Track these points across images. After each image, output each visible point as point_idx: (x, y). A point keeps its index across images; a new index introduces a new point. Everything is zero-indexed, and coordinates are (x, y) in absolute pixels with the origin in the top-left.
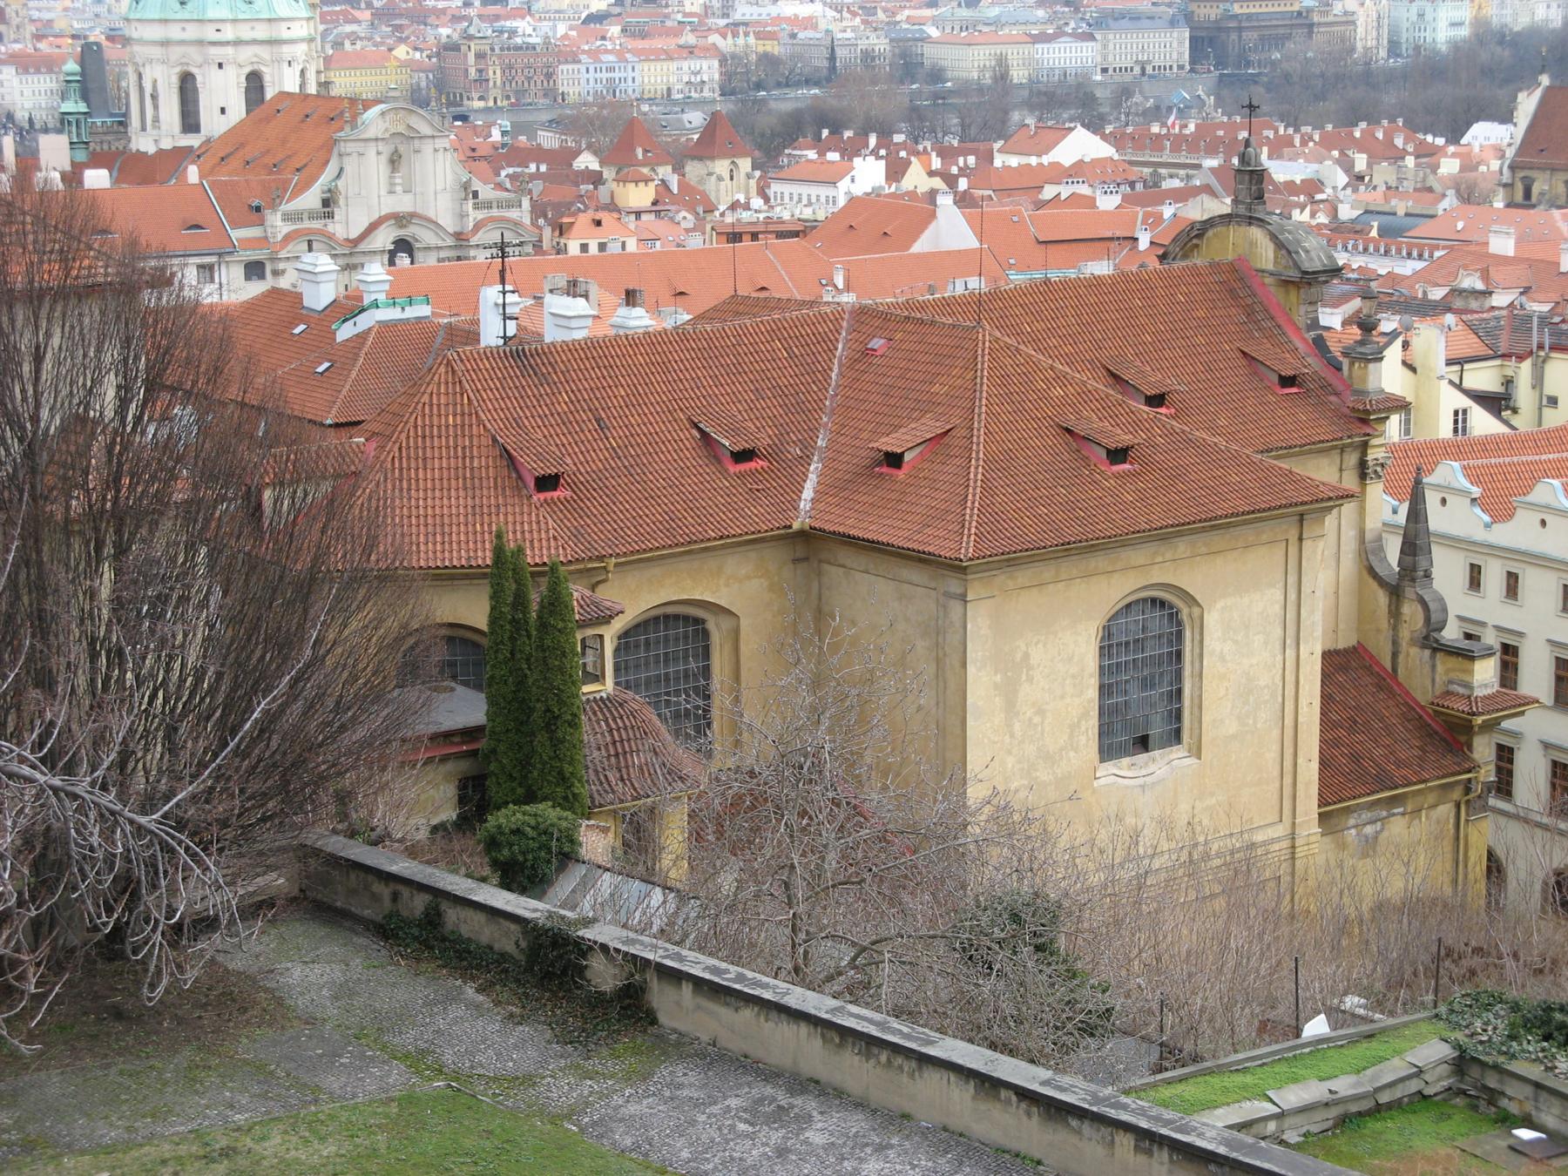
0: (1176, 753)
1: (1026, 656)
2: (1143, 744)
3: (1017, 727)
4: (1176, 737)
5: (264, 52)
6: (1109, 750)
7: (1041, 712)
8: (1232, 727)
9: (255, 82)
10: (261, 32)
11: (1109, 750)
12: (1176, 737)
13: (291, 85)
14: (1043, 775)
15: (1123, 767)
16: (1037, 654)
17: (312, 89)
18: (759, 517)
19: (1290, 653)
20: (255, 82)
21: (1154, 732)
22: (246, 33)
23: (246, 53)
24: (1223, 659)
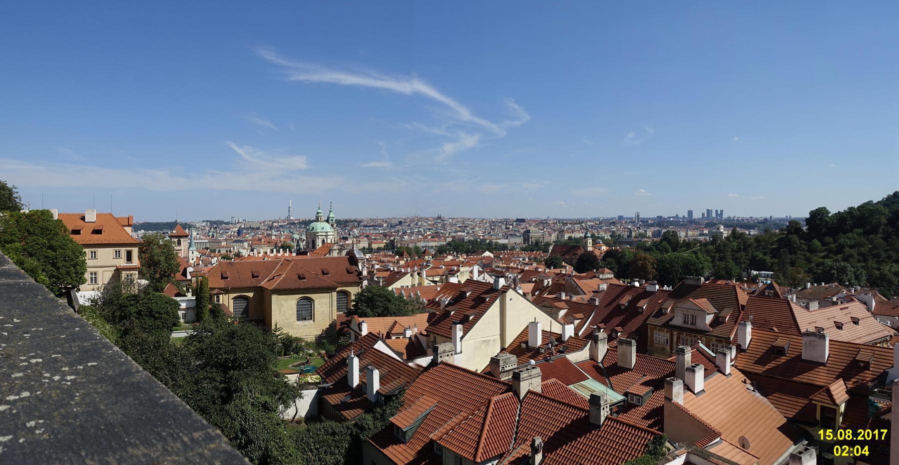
0: (311, 321)
1: (283, 304)
2: (305, 319)
3: (281, 314)
4: (311, 319)
5: (325, 237)
6: (297, 320)
7: (286, 313)
8: (321, 319)
9: (323, 241)
10: (325, 234)
11: (297, 320)
12: (311, 319)
13: (329, 241)
14: (286, 322)
15: (301, 323)
16: (285, 304)
17: (333, 242)
18: (254, 284)
19: (331, 309)
20: (323, 241)
21: (307, 318)
22: (322, 234)
23: (322, 237)
24: (318, 308)
